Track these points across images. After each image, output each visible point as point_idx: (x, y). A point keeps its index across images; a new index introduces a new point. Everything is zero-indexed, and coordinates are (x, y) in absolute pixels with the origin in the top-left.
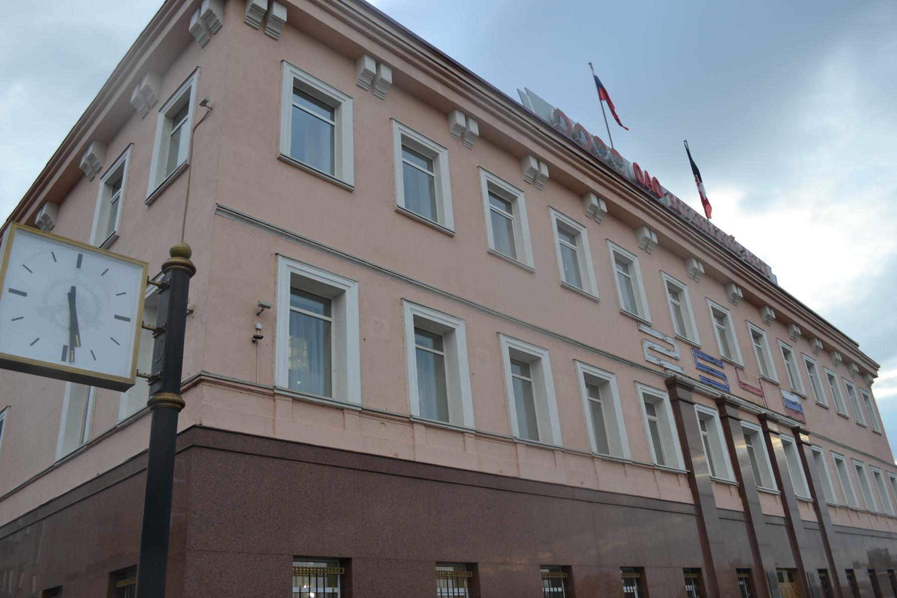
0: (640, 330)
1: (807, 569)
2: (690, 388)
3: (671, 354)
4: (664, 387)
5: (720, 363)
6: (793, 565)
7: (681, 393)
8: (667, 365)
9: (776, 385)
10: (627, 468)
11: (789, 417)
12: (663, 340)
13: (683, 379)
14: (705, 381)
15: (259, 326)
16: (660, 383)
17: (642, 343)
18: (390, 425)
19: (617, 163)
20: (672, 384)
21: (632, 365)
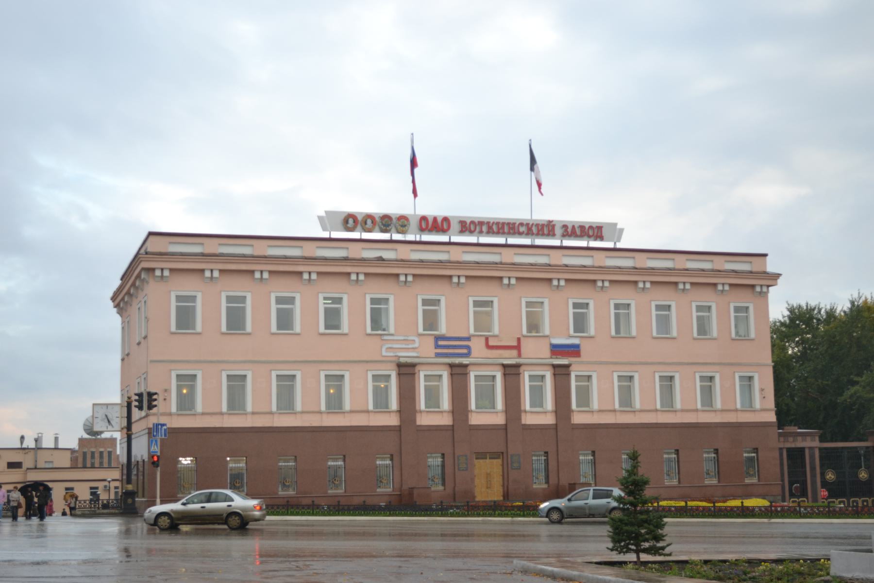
0: (382, 340)
1: (511, 452)
2: (413, 365)
3: (410, 346)
4: (395, 367)
5: (468, 339)
6: (503, 449)
7: (404, 370)
9: (547, 336)
10: (346, 414)
11: (551, 358)
12: (404, 340)
14: (438, 355)
15: (166, 395)
17: (381, 347)
20: (400, 366)
21: (367, 362)
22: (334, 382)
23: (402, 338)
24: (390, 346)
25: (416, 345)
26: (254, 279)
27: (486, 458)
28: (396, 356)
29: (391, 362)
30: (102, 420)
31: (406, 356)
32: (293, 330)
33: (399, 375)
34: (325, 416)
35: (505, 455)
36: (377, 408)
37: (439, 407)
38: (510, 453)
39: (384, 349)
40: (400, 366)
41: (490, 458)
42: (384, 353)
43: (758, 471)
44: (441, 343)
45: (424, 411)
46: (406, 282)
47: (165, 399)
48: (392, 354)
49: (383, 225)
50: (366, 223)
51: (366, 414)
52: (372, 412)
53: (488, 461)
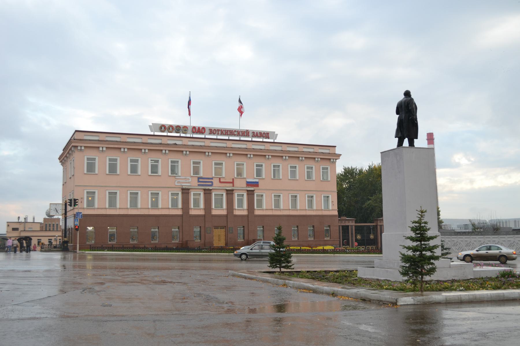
2: (189, 189)
3: (187, 181)
5: (212, 179)
6: (226, 225)
7: (184, 191)
8: (183, 184)
9: (245, 178)
10: (159, 209)
11: (246, 187)
13: (186, 188)
14: (199, 185)
16: (180, 189)
18: (103, 210)
19: (185, 131)
20: (183, 189)
21: (169, 187)
22: (155, 196)
23: (184, 178)
24: (178, 181)
25: (190, 181)
26: (121, 151)
27: (218, 229)
28: (181, 185)
29: (179, 188)
30: (54, 210)
31: (186, 185)
32: (137, 173)
33: (182, 193)
34: (150, 210)
35: (226, 227)
36: (173, 207)
37: (199, 207)
38: (228, 226)
39: (176, 182)
40: (183, 189)
41: (220, 229)
42: (176, 184)
43: (330, 235)
44: (200, 180)
45: (193, 209)
46: (186, 154)
47: (81, 202)
48: (179, 185)
49: (176, 129)
50: (169, 129)
51: (168, 210)
52: (170, 209)
53: (219, 230)
